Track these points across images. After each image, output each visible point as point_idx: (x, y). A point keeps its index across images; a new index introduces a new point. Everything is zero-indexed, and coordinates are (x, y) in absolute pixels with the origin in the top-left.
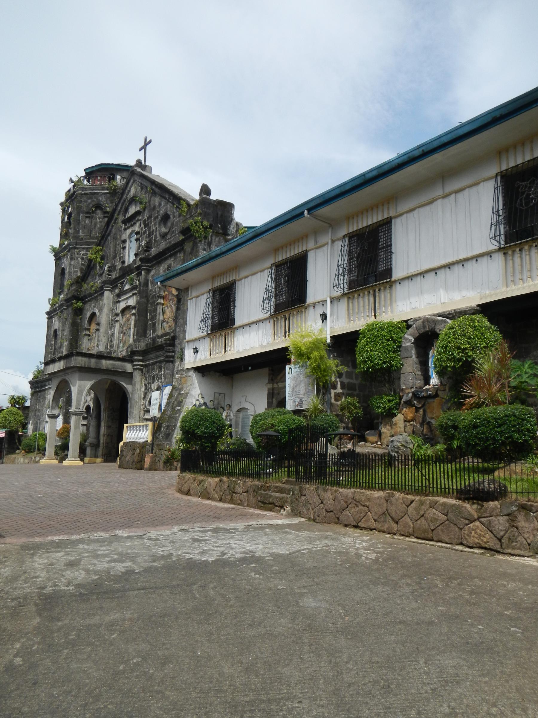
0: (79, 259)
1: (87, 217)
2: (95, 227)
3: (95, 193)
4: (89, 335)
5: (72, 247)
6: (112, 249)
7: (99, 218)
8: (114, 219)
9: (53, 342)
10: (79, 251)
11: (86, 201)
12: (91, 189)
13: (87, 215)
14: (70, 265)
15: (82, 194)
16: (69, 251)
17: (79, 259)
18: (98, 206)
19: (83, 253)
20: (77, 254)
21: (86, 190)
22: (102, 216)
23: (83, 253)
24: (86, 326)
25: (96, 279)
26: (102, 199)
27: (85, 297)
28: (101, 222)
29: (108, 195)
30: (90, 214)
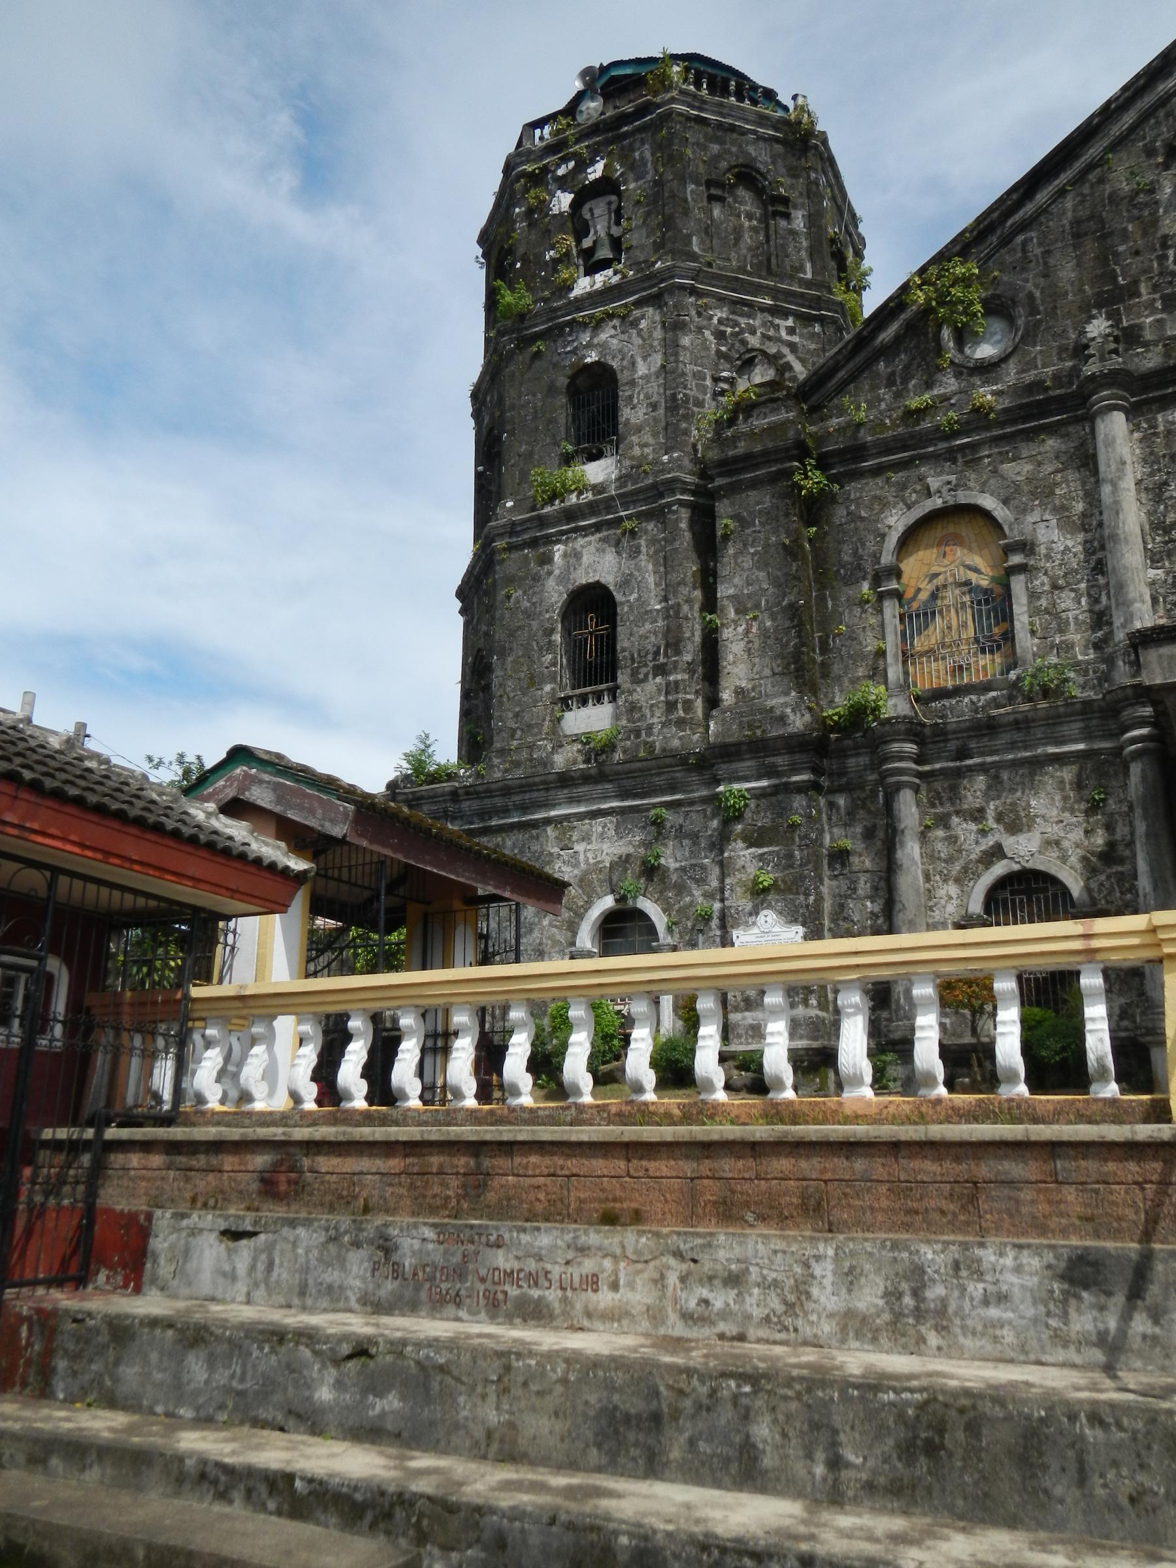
0: (707, 333)
1: (711, 198)
2: (737, 240)
3: (732, 128)
4: (898, 595)
5: (682, 287)
6: (1067, 272)
7: (750, 217)
8: (1079, 165)
9: (557, 638)
10: (707, 307)
11: (705, 148)
12: (720, 109)
13: (713, 191)
14: (671, 348)
15: (688, 118)
16: (655, 300)
17: (707, 333)
18: (748, 176)
19: (719, 314)
20: (699, 314)
21: (701, 109)
22: (758, 213)
23: (719, 314)
24: (887, 559)
25: (929, 385)
26: (761, 155)
27: (857, 452)
28: (752, 228)
29: (779, 148)
30: (716, 189)
